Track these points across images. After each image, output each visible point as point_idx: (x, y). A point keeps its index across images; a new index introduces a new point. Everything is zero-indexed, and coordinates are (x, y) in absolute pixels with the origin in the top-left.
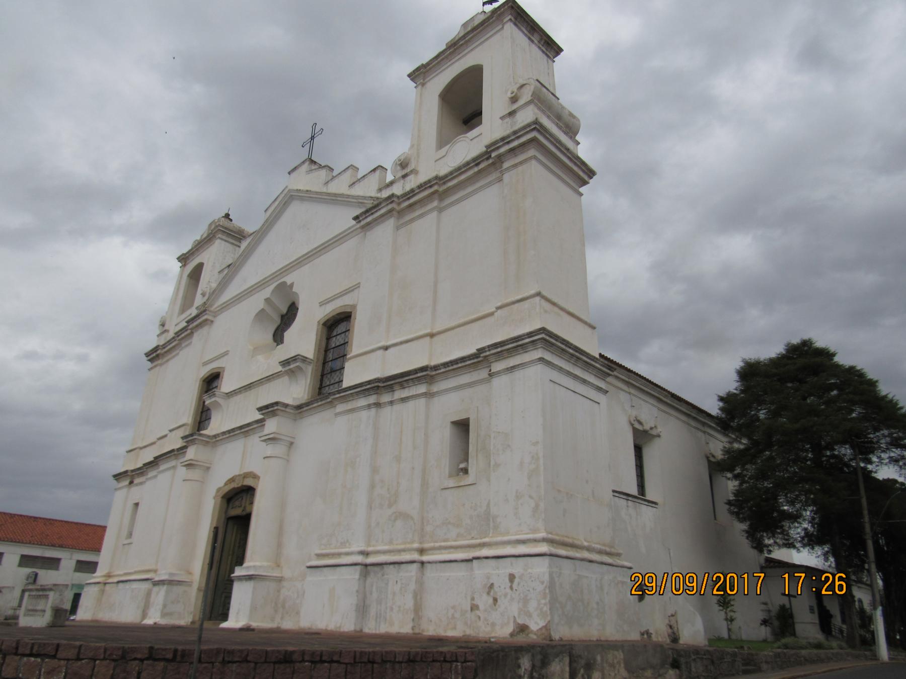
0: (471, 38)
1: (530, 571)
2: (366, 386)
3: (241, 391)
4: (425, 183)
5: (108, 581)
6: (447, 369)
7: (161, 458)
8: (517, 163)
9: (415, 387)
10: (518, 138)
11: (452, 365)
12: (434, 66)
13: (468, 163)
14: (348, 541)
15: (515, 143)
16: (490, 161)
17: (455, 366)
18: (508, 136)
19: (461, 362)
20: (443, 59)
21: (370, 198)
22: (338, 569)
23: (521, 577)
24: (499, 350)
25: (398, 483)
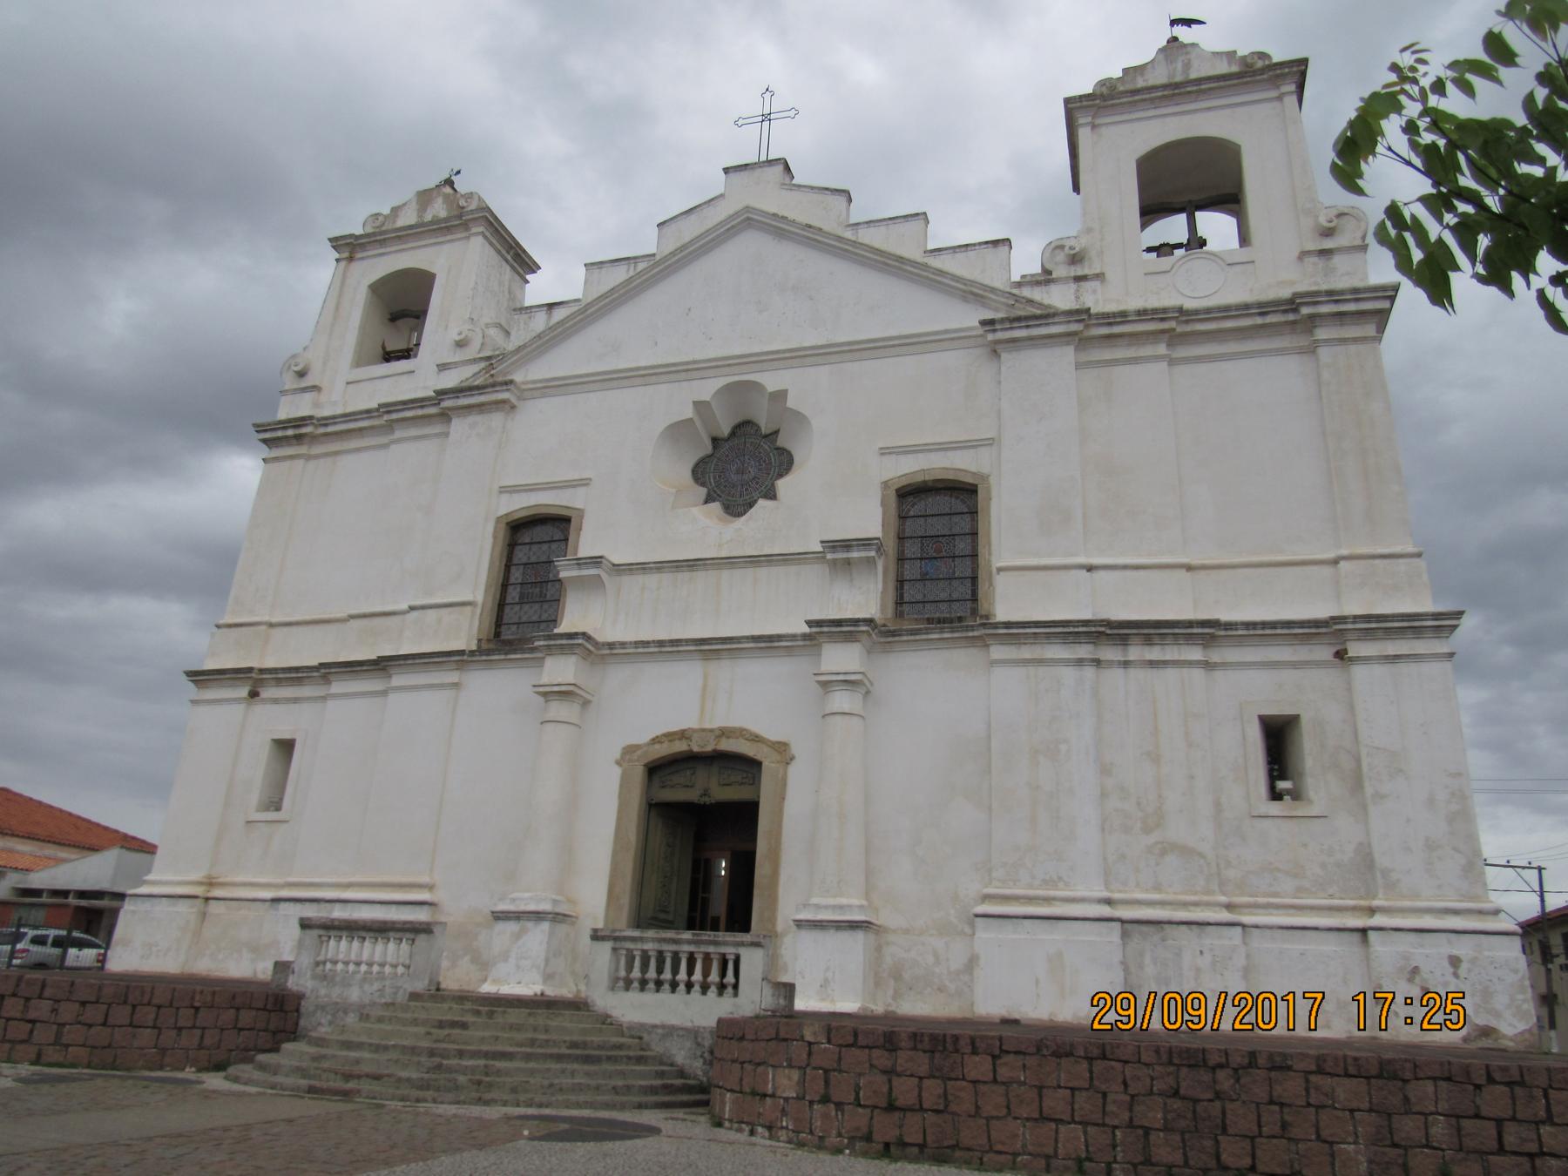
0: (1210, 89)
1: (1486, 953)
2: (1074, 626)
3: (663, 567)
4: (1155, 311)
6: (1252, 632)
7: (398, 663)
8: (1348, 338)
9: (1175, 647)
10: (1357, 300)
11: (1263, 629)
12: (1121, 104)
13: (1247, 306)
14: (1060, 878)
15: (1351, 307)
16: (1291, 317)
18: (1342, 292)
20: (1145, 100)
21: (1007, 295)
23: (1473, 961)
24: (1373, 625)
25: (1160, 796)
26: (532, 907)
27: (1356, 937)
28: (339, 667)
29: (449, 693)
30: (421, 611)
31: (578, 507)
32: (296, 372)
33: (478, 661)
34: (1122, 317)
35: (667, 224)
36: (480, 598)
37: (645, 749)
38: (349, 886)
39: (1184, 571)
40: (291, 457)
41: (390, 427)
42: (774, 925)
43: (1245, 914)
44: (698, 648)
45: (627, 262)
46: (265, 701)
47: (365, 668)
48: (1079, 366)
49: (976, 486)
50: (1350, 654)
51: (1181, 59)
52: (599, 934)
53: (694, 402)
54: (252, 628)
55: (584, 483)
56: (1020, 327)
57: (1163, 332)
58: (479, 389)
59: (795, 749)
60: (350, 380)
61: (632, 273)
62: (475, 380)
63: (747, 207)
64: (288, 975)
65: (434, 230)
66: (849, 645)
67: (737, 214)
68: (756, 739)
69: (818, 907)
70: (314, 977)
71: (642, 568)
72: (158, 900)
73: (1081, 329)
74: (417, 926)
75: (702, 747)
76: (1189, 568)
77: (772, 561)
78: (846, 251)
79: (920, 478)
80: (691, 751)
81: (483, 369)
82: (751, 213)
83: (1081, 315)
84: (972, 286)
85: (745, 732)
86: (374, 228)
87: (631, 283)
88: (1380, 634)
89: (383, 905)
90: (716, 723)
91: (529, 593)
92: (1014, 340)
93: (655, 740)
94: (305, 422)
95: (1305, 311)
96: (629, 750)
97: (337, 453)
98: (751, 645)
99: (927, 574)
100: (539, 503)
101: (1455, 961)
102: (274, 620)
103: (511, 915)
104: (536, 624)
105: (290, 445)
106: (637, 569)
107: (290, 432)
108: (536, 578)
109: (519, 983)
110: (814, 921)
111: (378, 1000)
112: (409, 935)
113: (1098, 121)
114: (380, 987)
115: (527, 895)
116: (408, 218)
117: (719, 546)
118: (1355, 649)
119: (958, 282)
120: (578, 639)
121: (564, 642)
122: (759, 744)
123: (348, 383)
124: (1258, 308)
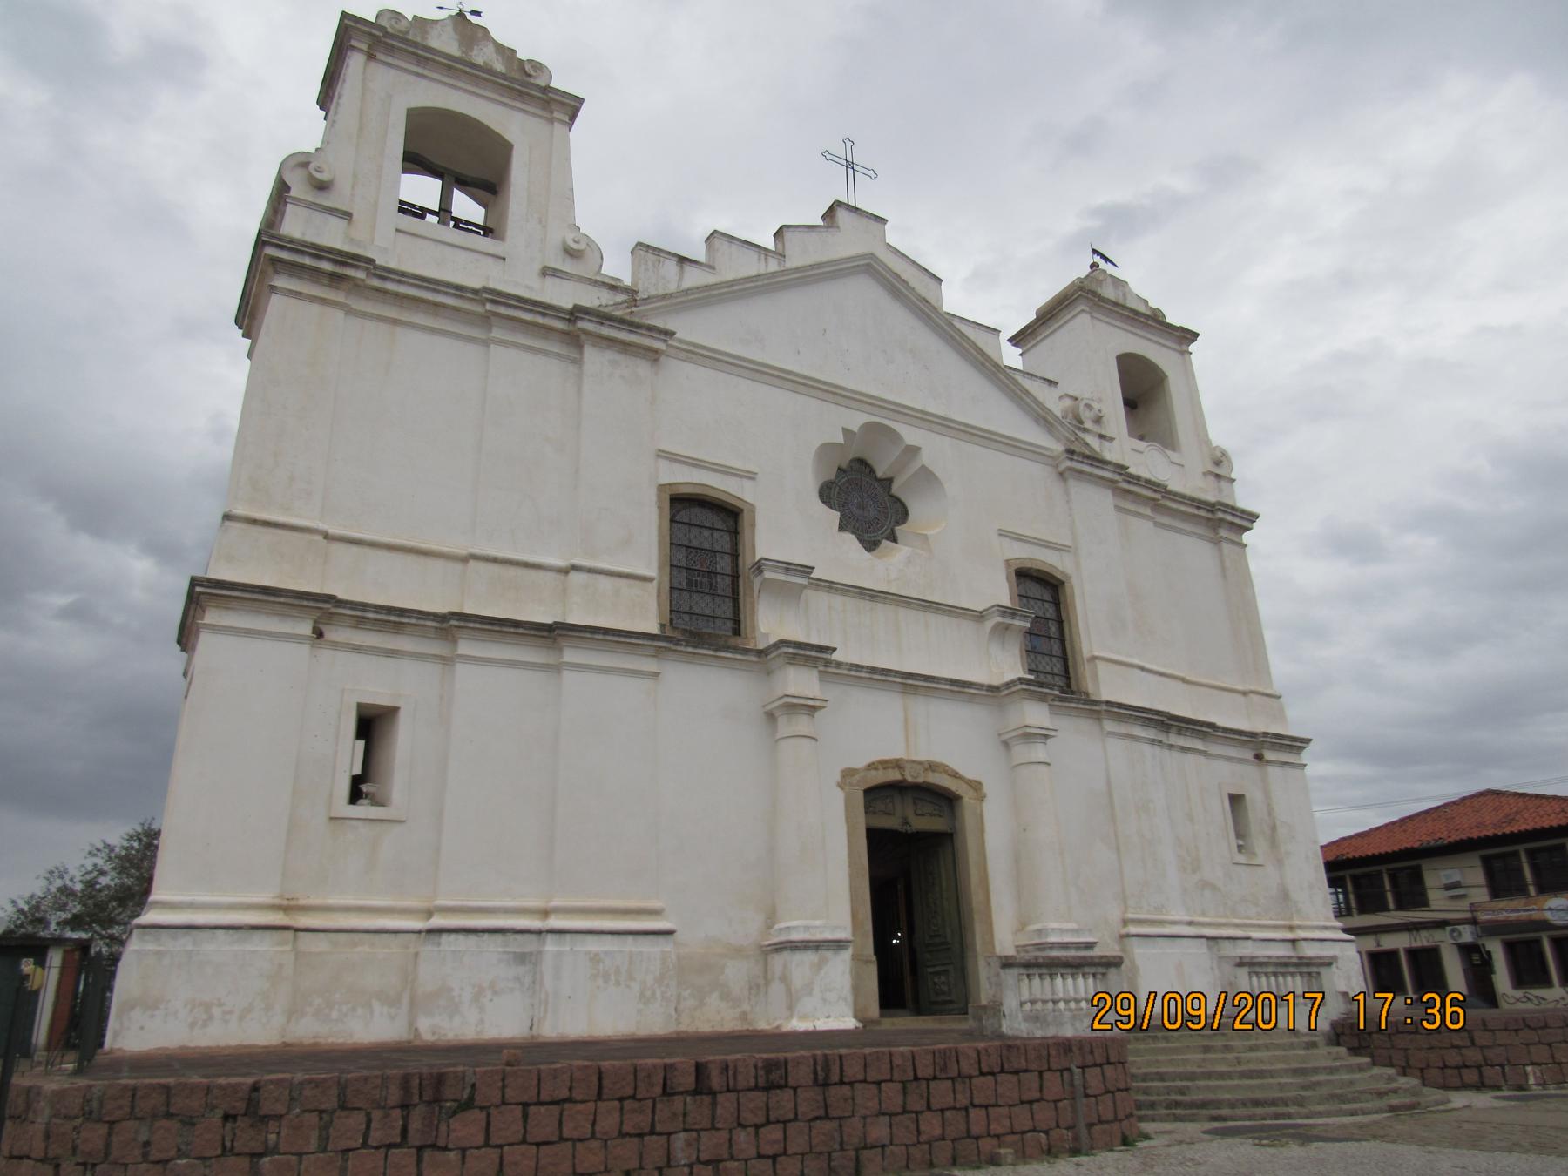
0: (1151, 325)
2: (1153, 714)
4: (1154, 483)
7: (582, 635)
10: (1241, 518)
13: (1193, 499)
15: (1237, 521)
16: (1210, 515)
20: (1117, 312)
22: (1178, 940)
26: (829, 936)
27: (1289, 945)
28: (481, 623)
29: (646, 684)
30: (590, 575)
31: (749, 501)
33: (681, 651)
34: (1135, 479)
35: (791, 229)
36: (652, 572)
37: (862, 774)
38: (545, 913)
40: (323, 301)
41: (486, 320)
43: (1251, 931)
44: (904, 681)
45: (757, 250)
46: (335, 645)
47: (521, 631)
48: (1118, 508)
49: (1063, 583)
52: (1245, 960)
53: (843, 429)
55: (750, 476)
56: (1087, 463)
57: (1154, 499)
58: (634, 326)
59: (986, 789)
60: (400, 228)
61: (762, 270)
62: (613, 311)
63: (872, 254)
64: (999, 1021)
65: (502, 85)
66: (1041, 703)
68: (956, 775)
69: (1061, 931)
70: (1027, 1019)
71: (829, 586)
72: (207, 934)
73: (1120, 480)
74: (1112, 960)
75: (916, 778)
76: (1183, 680)
77: (930, 607)
78: (952, 337)
79: (1029, 565)
82: (875, 262)
83: (1121, 469)
84: (1047, 413)
87: (775, 277)
89: (616, 936)
90: (922, 756)
91: (696, 581)
92: (1081, 472)
93: (872, 766)
94: (355, 263)
95: (1220, 515)
96: (848, 773)
97: (395, 322)
98: (947, 687)
102: (334, 530)
104: (711, 619)
106: (825, 586)
107: (327, 266)
108: (702, 566)
109: (828, 1017)
112: (1101, 970)
115: (818, 923)
116: (446, 43)
118: (1269, 755)
119: (1038, 406)
121: (813, 654)
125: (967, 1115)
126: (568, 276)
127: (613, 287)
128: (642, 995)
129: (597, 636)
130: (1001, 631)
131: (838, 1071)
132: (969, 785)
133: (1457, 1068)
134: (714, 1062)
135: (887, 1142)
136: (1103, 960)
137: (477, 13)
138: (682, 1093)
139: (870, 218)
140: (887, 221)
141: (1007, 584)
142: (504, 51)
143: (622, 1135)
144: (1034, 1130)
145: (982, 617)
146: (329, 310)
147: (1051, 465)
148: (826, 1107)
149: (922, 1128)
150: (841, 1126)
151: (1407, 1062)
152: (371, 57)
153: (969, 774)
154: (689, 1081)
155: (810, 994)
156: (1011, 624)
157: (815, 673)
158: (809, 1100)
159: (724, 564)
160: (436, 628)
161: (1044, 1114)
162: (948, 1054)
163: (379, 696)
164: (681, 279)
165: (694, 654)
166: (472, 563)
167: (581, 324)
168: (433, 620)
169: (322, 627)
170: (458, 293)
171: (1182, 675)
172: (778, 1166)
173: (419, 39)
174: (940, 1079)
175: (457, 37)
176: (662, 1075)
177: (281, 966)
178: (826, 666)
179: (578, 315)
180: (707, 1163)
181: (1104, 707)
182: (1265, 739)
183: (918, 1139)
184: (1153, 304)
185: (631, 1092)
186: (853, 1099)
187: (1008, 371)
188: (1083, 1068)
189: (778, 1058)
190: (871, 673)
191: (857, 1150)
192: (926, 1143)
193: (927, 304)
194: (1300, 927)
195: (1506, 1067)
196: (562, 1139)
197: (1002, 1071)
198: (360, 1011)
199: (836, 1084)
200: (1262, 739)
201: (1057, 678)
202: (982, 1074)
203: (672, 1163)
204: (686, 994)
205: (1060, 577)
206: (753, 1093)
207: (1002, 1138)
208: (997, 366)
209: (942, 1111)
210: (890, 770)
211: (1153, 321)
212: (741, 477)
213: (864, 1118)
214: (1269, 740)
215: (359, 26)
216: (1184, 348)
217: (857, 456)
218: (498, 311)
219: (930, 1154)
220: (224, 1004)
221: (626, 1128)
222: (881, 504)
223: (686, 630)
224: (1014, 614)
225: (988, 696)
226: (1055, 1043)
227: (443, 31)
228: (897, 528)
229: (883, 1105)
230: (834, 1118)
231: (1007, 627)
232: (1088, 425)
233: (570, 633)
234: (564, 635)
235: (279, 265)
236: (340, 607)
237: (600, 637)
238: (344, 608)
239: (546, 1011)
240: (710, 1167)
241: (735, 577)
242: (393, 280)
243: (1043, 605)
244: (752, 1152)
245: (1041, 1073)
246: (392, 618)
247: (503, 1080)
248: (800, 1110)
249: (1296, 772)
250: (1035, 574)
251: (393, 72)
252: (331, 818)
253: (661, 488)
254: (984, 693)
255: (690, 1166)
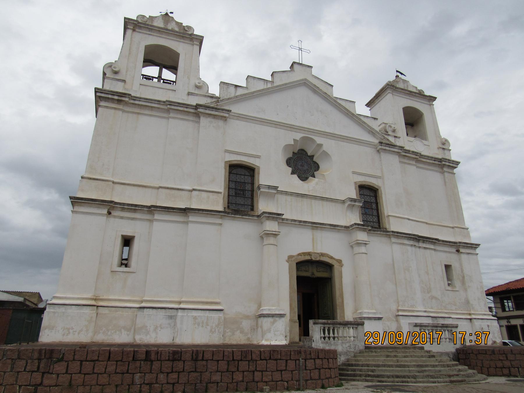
2: (412, 236)
4: (416, 153)
5: (98, 305)
6: (443, 243)
10: (453, 163)
12: (399, 91)
13: (432, 158)
14: (414, 305)
15: (451, 165)
16: (440, 163)
17: (446, 243)
19: (448, 243)
22: (419, 317)
24: (465, 245)
25: (430, 284)
26: (277, 312)
27: (469, 320)
28: (161, 208)
30: (200, 192)
31: (257, 165)
32: (113, 70)
33: (230, 216)
34: (408, 151)
35: (277, 73)
36: (222, 190)
37: (296, 257)
38: (180, 303)
39: (426, 224)
40: (115, 109)
41: (168, 111)
42: (344, 318)
43: (452, 315)
44: (312, 225)
45: (263, 81)
46: (115, 217)
47: (175, 211)
48: (400, 162)
49: (378, 189)
50: (461, 251)
51: (406, 83)
52: (417, 325)
54: (104, 182)
55: (258, 157)
56: (388, 147)
57: (416, 158)
58: (217, 109)
59: (343, 262)
61: (265, 87)
62: (211, 105)
63: (306, 79)
67: (302, 80)
68: (332, 258)
70: (322, 343)
71: (286, 193)
73: (402, 152)
74: (359, 323)
75: (316, 259)
76: (427, 223)
78: (336, 105)
79: (364, 184)
80: (312, 259)
81: (215, 101)
82: (307, 81)
83: (402, 148)
85: (328, 255)
86: (142, 20)
87: (269, 90)
88: (466, 247)
92: (385, 150)
93: (299, 255)
95: (444, 163)
96: (290, 257)
97: (138, 113)
98: (329, 227)
99: (366, 213)
100: (241, 160)
101: (488, 326)
102: (115, 181)
103: (270, 315)
104: (243, 206)
105: (113, 103)
106: (284, 193)
107: (116, 97)
109: (276, 340)
110: (369, 317)
111: (349, 350)
112: (355, 326)
113: (394, 93)
114: (349, 345)
115: (274, 308)
116: (159, 24)
117: (309, 191)
118: (462, 250)
119: (369, 127)
120: (280, 216)
121: (275, 216)
122: (333, 259)
123: (140, 84)
124: (434, 159)
125: (254, 374)
126: (197, 95)
127: (212, 97)
128: (211, 331)
129: (200, 212)
130: (351, 207)
131: (202, 356)
132: (337, 261)
133: (501, 368)
134: (153, 350)
135: (219, 381)
136: (356, 323)
137: (172, 13)
138: (140, 360)
139: (306, 67)
140: (313, 67)
141: (355, 191)
142: (178, 24)
143: (116, 373)
144: (282, 381)
145: (344, 202)
146: (117, 112)
147: (375, 148)
148: (196, 368)
149: (234, 377)
150: (201, 375)
151: (483, 365)
152: (134, 30)
153: (337, 257)
154: (143, 356)
155: (270, 332)
156: (355, 205)
157: (277, 223)
158: (189, 365)
159: (248, 187)
160: (147, 210)
161: (287, 376)
162: (248, 352)
163: (128, 233)
164: (235, 93)
165: (235, 217)
166: (160, 189)
167: (199, 110)
168: (146, 208)
169: (111, 211)
170: (159, 103)
171: (426, 221)
172: (175, 387)
173: (150, 24)
174: (244, 360)
175: (163, 21)
176: (133, 354)
177: (92, 317)
178: (282, 220)
179: (198, 107)
180: (147, 384)
181: (391, 233)
182: (460, 244)
183: (232, 381)
184: (419, 88)
185: (120, 359)
186: (207, 366)
187: (357, 115)
188: (305, 360)
189: (178, 350)
190: (300, 222)
191: (207, 383)
192: (235, 383)
193: (326, 95)
194: (473, 314)
195: (520, 369)
196: (94, 373)
197: (270, 359)
198: (118, 332)
199: (200, 360)
200: (459, 244)
201: (375, 224)
202: (261, 359)
203: (134, 383)
204: (228, 331)
205: (376, 187)
206: (167, 362)
207: (268, 383)
208: (353, 114)
209: (243, 372)
210: (306, 256)
211: (420, 95)
212: (255, 157)
213: (211, 372)
214: (462, 245)
215: (130, 21)
216: (431, 103)
217: (301, 148)
218: (171, 108)
219: (237, 386)
220: (73, 329)
221: (117, 371)
222: (309, 164)
223: (233, 209)
224: (355, 201)
225: (344, 230)
226: (294, 350)
227: (158, 20)
228: (315, 173)
229: (219, 369)
230: (199, 372)
231: (353, 206)
232: (390, 133)
233: (191, 211)
234: (189, 212)
235: (101, 99)
236: (116, 205)
237: (201, 212)
238: (117, 205)
239: (177, 335)
240: (148, 386)
241: (252, 191)
242: (137, 100)
243: (370, 197)
244: (165, 381)
245: (287, 361)
246: (133, 208)
247: (74, 353)
248: (185, 368)
249: (474, 257)
250: (367, 187)
251: (141, 34)
252: (112, 271)
253: (226, 162)
254: (343, 229)
255: (141, 385)
